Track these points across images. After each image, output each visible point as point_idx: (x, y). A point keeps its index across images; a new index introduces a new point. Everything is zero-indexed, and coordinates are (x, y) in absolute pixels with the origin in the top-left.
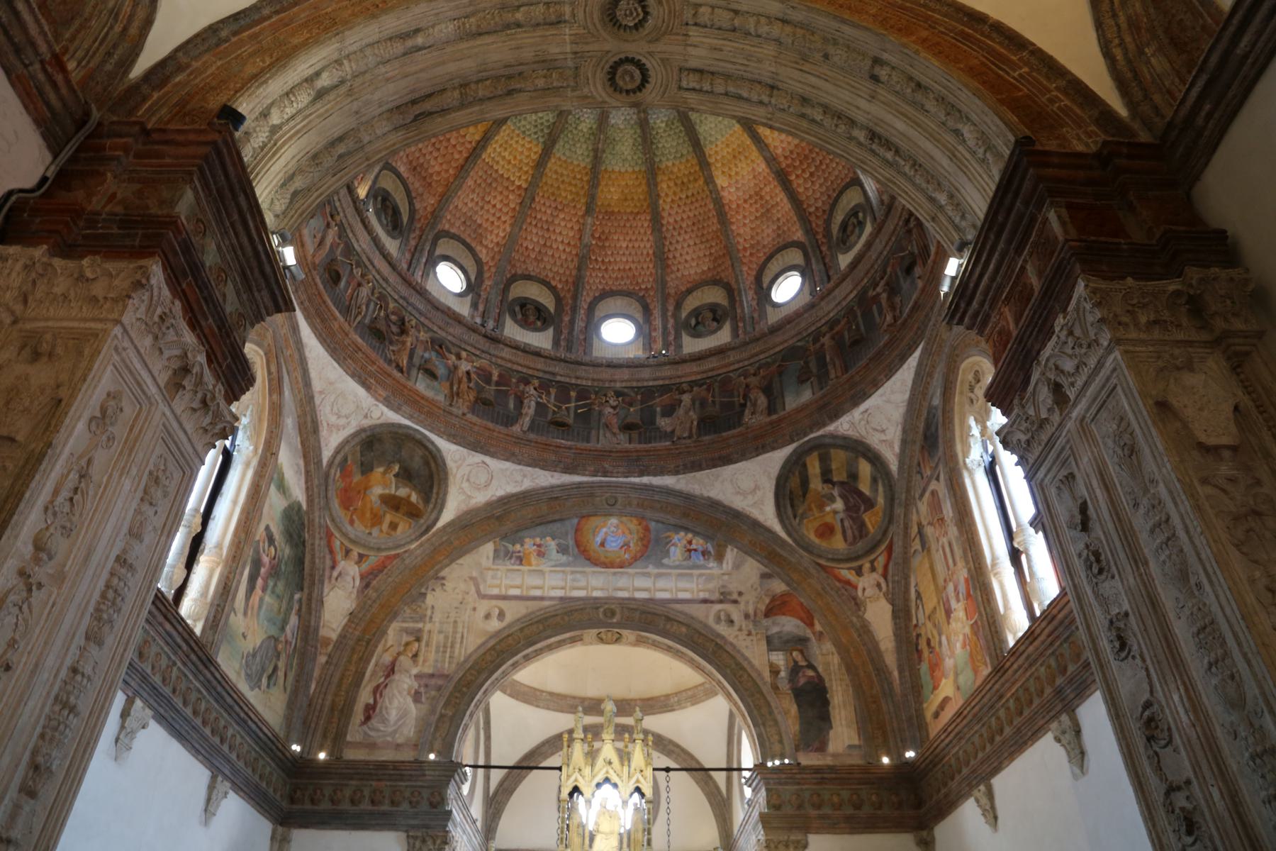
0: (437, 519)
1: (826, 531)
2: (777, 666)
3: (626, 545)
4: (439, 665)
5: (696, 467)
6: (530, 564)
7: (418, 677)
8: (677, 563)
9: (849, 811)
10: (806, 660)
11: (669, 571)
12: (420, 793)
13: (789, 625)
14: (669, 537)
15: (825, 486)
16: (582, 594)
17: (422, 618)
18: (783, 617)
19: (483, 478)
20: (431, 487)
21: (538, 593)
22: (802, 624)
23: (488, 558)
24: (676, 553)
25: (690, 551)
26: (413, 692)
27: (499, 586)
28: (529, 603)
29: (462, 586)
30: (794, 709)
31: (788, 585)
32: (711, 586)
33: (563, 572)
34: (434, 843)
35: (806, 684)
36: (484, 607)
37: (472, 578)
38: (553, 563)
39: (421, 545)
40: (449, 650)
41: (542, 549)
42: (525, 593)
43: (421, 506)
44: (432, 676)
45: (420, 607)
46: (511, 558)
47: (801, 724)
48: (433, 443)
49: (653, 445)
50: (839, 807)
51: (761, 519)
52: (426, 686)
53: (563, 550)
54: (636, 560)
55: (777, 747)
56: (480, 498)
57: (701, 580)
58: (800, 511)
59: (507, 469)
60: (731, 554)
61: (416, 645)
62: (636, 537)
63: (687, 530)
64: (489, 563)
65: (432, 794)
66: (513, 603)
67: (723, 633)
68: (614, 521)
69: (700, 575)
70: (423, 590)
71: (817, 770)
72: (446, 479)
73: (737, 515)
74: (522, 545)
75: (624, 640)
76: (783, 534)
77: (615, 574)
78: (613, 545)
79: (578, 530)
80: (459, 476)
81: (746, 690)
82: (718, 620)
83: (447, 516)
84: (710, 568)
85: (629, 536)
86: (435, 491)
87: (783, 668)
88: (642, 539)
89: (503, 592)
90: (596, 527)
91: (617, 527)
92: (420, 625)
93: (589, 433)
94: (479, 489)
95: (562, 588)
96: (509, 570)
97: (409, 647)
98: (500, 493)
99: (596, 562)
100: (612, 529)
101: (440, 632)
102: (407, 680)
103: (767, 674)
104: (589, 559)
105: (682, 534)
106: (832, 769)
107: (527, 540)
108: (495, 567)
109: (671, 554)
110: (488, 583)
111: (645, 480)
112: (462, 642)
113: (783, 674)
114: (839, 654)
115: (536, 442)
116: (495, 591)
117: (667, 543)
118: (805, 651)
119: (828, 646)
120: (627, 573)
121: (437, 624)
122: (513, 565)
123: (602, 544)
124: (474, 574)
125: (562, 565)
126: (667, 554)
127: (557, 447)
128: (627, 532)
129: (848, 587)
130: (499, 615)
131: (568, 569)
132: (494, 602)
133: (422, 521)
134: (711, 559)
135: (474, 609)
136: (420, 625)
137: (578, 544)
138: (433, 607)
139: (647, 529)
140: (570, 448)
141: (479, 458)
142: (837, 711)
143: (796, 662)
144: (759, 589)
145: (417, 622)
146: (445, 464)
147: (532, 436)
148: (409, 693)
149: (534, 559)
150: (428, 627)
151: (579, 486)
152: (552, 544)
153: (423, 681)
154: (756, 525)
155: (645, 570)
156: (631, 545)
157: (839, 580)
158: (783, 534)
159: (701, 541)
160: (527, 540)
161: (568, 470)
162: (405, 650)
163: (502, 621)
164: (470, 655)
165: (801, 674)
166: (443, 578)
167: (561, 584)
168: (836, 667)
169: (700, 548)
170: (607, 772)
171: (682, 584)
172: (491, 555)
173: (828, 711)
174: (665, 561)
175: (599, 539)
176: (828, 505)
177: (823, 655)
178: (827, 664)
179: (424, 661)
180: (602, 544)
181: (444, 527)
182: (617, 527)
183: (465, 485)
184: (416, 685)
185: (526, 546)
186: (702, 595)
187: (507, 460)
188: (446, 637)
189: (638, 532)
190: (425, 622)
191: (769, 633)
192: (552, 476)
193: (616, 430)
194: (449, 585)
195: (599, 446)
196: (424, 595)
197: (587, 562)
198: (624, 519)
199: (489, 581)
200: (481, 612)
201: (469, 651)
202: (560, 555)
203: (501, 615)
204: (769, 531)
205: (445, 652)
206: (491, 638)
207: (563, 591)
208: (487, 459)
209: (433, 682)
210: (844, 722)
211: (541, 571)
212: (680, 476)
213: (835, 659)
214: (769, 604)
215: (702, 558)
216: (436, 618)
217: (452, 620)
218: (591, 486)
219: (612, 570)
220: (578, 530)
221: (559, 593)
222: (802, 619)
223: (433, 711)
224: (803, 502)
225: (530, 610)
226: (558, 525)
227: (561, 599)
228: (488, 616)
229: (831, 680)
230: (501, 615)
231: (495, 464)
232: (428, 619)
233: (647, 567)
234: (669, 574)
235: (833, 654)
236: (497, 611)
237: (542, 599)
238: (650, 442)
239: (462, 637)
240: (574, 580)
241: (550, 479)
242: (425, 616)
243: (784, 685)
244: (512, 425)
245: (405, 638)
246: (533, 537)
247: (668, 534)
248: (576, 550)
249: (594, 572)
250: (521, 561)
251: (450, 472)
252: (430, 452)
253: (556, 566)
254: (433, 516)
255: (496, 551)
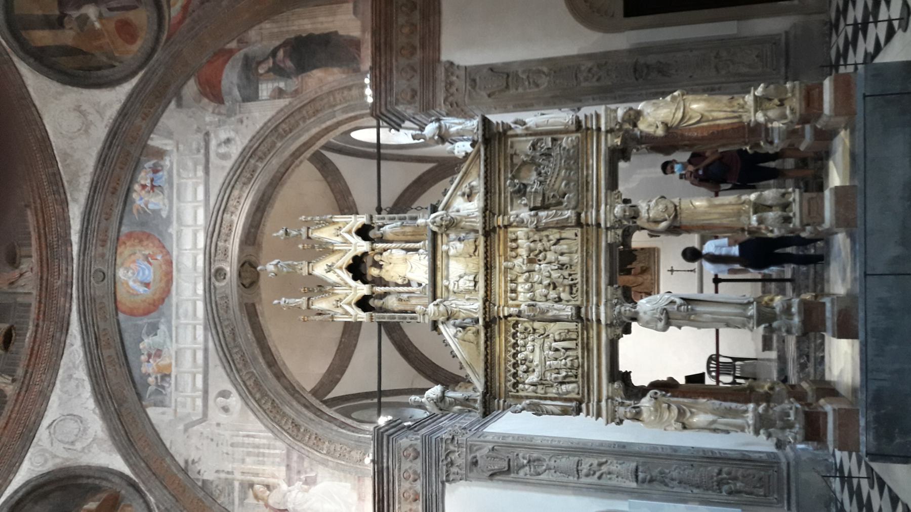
0: (121, 475)
1: (127, 31)
2: (274, 90)
3: (146, 258)
4: (278, 460)
5: (56, 180)
6: (170, 365)
7: (290, 482)
8: (166, 201)
9: (417, 16)
10: (267, 58)
11: (175, 209)
12: (406, 471)
13: (230, 77)
14: (138, 210)
15: (68, 27)
16: (200, 306)
17: (230, 483)
18: (223, 83)
19: (72, 426)
20: (79, 486)
21: (200, 355)
22: (230, 62)
23: (163, 413)
24: (155, 202)
25: (153, 187)
26: (306, 487)
27: (194, 399)
28: (211, 365)
29: (194, 441)
30: (317, 74)
31: (188, 78)
32: (190, 164)
33: (177, 328)
34: (454, 452)
35: (291, 60)
36: (216, 415)
37: (186, 430)
38: (168, 340)
39: (150, 490)
40: (262, 450)
41: (153, 352)
42: (201, 370)
43: (104, 496)
44: (288, 466)
45: (217, 486)
46: (163, 388)
47: (332, 66)
48: (16, 492)
49: (31, 229)
50: (413, 25)
51: (117, 107)
52: (299, 472)
53: (153, 329)
54: (164, 247)
55: (355, 92)
56: (96, 425)
57: (184, 174)
58: (105, 59)
59: (60, 398)
60: (156, 141)
61: (257, 487)
62: (138, 248)
63: (129, 191)
64: (170, 411)
65: (406, 457)
66: (211, 382)
67: (240, 150)
68: (121, 273)
69: (179, 175)
70: (200, 484)
71: (377, 49)
72: (68, 469)
73: (114, 134)
74: (149, 375)
75: (253, 259)
76: (134, 81)
77: (179, 271)
78: (149, 273)
79: (132, 313)
80: (66, 455)
81: (298, 125)
82: (224, 157)
83: (118, 463)
84: (172, 164)
85: (138, 255)
86: (85, 481)
87: (276, 85)
88: (141, 241)
89: (200, 393)
90: (128, 292)
91: (128, 269)
92: (237, 484)
93: (21, 305)
94: (85, 430)
95: (195, 328)
96: (176, 389)
97: (260, 494)
98: (91, 404)
99: (166, 292)
100: (130, 274)
101: (243, 461)
102: (294, 494)
103: (282, 103)
104: (163, 300)
105: (134, 195)
106: (375, 33)
107: (144, 370)
108: (173, 404)
109: (156, 207)
110: (190, 411)
111: (75, 238)
112: (253, 436)
113: (282, 85)
114: (261, 22)
115: (28, 366)
116: (199, 402)
117: (145, 212)
118: (259, 59)
119: (253, 34)
120: (178, 257)
121: (235, 465)
122: (170, 384)
123: (147, 285)
124: (181, 427)
125: (170, 330)
126: (157, 213)
127: (34, 342)
128: (133, 257)
129: (190, 9)
130: (223, 397)
131: (174, 323)
132: (211, 402)
133: (123, 492)
134: (162, 163)
135: (218, 425)
136: (237, 484)
137: (147, 313)
138: (217, 471)
139: (130, 236)
140: (37, 326)
141: (43, 433)
142: (319, 26)
143: (269, 70)
144: (193, 109)
145: (233, 488)
146: (48, 473)
147: (20, 372)
148: (306, 491)
149: (163, 362)
150: (238, 476)
151: (82, 314)
152: (147, 342)
153: (295, 477)
154: (124, 113)
155: (175, 237)
156: (147, 252)
157: (184, 18)
158: (134, 81)
159: (143, 174)
160: (144, 370)
161: (65, 327)
162: (263, 499)
163: (230, 393)
164: (266, 426)
165: (282, 65)
166: (186, 462)
167: (190, 329)
168: (274, 25)
169: (151, 175)
170: (341, 268)
171: (189, 196)
172: (160, 410)
173: (319, 36)
174: (164, 214)
175: (142, 289)
176: (93, 25)
177: (262, 40)
178: (272, 36)
179: (274, 477)
180: (147, 285)
181: (130, 465)
182: (128, 269)
183: (79, 446)
184: (298, 484)
185: (150, 371)
186: (200, 173)
187: (48, 399)
188: (249, 454)
189: (133, 246)
190: (233, 480)
191: (240, 99)
192: (72, 345)
193: (17, 273)
194: (194, 455)
195: (35, 292)
196: (204, 481)
197: (166, 300)
198: (119, 261)
199: (188, 409)
200: (222, 417)
201: (263, 428)
202: (159, 331)
203: (224, 394)
204: (131, 97)
205: (264, 455)
206: (247, 404)
207: (197, 326)
208: (45, 423)
209: (294, 465)
210: (330, 19)
211: (176, 353)
212: (69, 198)
213: (267, 26)
214: (208, 98)
215: (160, 173)
216: (229, 467)
217: (230, 449)
218: (82, 300)
219: (175, 273)
220: (132, 313)
221: (200, 331)
222: (226, 62)
223: (324, 463)
224: (93, 55)
225: (218, 362)
226: (126, 336)
227: (205, 329)
228: (226, 409)
229: (288, 32)
230: (224, 394)
231: (53, 412)
232: (230, 476)
233: (171, 235)
234: (178, 209)
235: (261, 29)
236: (220, 399)
237: (206, 350)
238: (29, 233)
239: (248, 436)
240: (186, 316)
241: (75, 346)
242: (226, 479)
243: (293, 84)
244: (5, 396)
245: (251, 500)
246: (140, 365)
247: (135, 211)
248: (153, 315)
249: (177, 294)
250: (166, 375)
251: (59, 467)
252: (28, 494)
253: (171, 336)
254: (117, 480)
255: (155, 405)
